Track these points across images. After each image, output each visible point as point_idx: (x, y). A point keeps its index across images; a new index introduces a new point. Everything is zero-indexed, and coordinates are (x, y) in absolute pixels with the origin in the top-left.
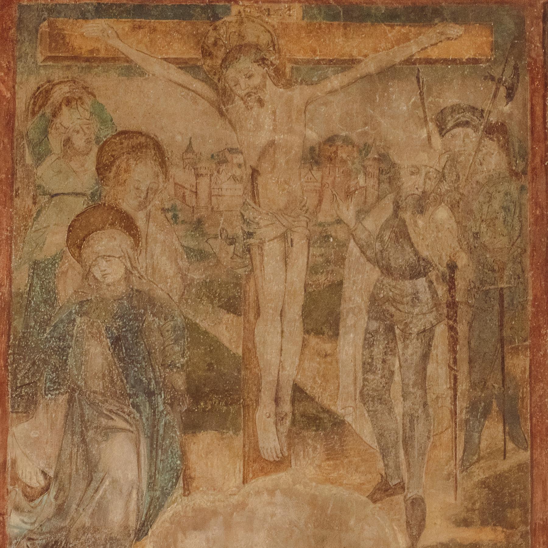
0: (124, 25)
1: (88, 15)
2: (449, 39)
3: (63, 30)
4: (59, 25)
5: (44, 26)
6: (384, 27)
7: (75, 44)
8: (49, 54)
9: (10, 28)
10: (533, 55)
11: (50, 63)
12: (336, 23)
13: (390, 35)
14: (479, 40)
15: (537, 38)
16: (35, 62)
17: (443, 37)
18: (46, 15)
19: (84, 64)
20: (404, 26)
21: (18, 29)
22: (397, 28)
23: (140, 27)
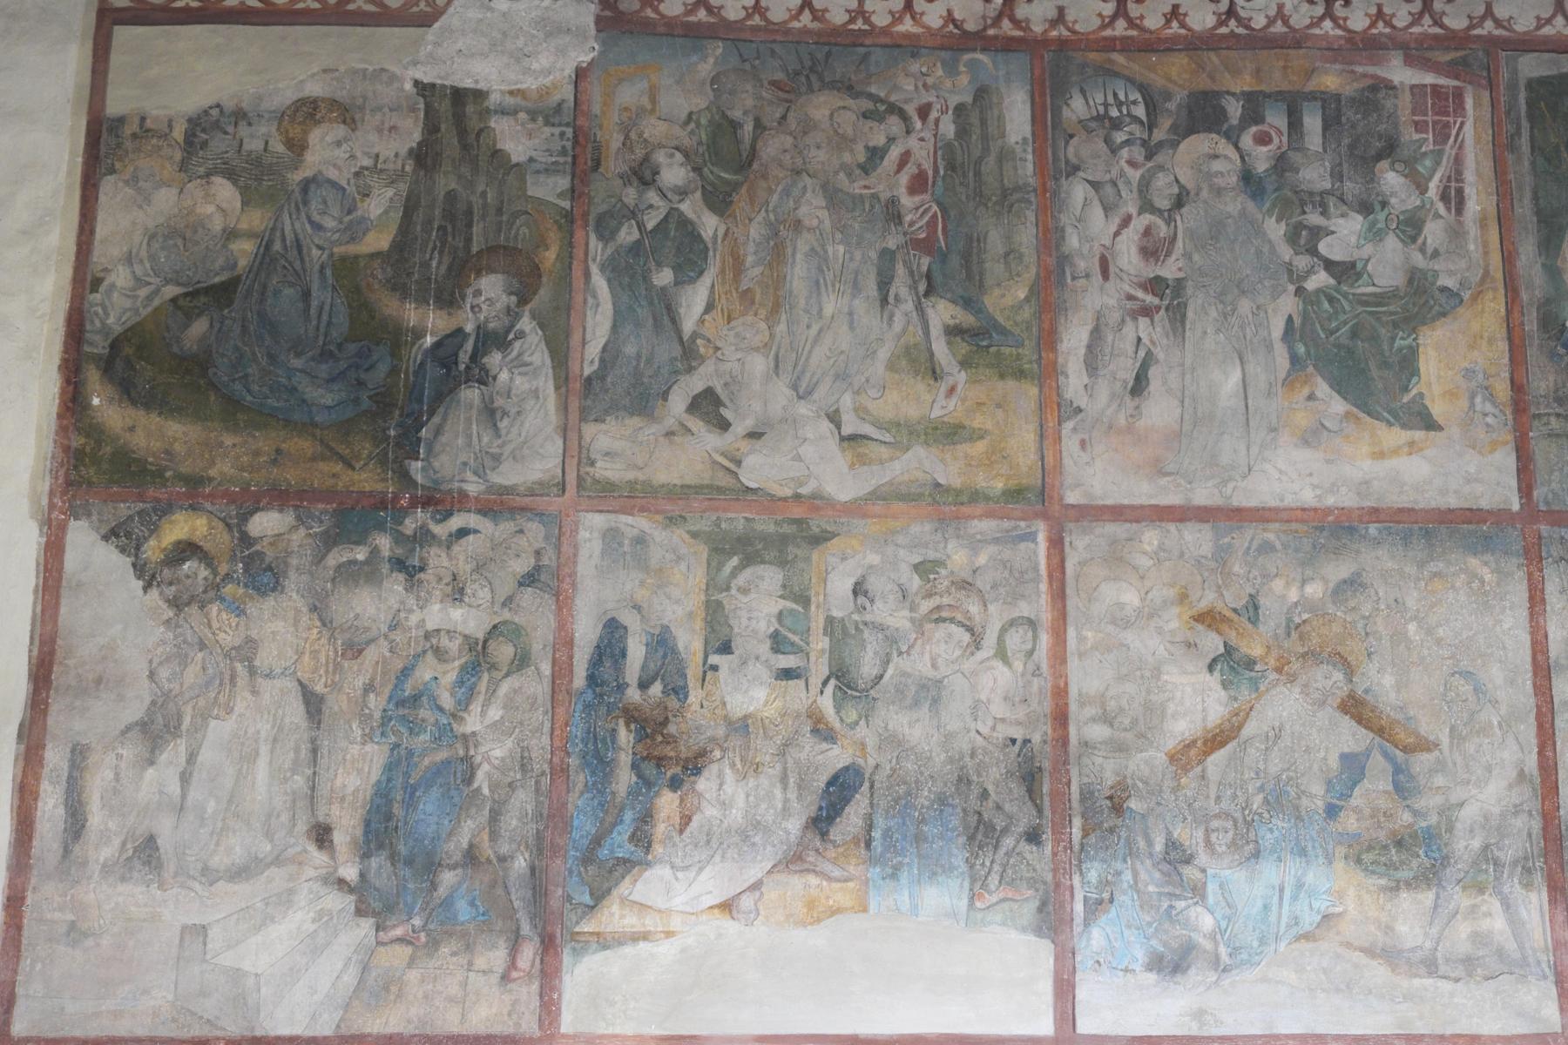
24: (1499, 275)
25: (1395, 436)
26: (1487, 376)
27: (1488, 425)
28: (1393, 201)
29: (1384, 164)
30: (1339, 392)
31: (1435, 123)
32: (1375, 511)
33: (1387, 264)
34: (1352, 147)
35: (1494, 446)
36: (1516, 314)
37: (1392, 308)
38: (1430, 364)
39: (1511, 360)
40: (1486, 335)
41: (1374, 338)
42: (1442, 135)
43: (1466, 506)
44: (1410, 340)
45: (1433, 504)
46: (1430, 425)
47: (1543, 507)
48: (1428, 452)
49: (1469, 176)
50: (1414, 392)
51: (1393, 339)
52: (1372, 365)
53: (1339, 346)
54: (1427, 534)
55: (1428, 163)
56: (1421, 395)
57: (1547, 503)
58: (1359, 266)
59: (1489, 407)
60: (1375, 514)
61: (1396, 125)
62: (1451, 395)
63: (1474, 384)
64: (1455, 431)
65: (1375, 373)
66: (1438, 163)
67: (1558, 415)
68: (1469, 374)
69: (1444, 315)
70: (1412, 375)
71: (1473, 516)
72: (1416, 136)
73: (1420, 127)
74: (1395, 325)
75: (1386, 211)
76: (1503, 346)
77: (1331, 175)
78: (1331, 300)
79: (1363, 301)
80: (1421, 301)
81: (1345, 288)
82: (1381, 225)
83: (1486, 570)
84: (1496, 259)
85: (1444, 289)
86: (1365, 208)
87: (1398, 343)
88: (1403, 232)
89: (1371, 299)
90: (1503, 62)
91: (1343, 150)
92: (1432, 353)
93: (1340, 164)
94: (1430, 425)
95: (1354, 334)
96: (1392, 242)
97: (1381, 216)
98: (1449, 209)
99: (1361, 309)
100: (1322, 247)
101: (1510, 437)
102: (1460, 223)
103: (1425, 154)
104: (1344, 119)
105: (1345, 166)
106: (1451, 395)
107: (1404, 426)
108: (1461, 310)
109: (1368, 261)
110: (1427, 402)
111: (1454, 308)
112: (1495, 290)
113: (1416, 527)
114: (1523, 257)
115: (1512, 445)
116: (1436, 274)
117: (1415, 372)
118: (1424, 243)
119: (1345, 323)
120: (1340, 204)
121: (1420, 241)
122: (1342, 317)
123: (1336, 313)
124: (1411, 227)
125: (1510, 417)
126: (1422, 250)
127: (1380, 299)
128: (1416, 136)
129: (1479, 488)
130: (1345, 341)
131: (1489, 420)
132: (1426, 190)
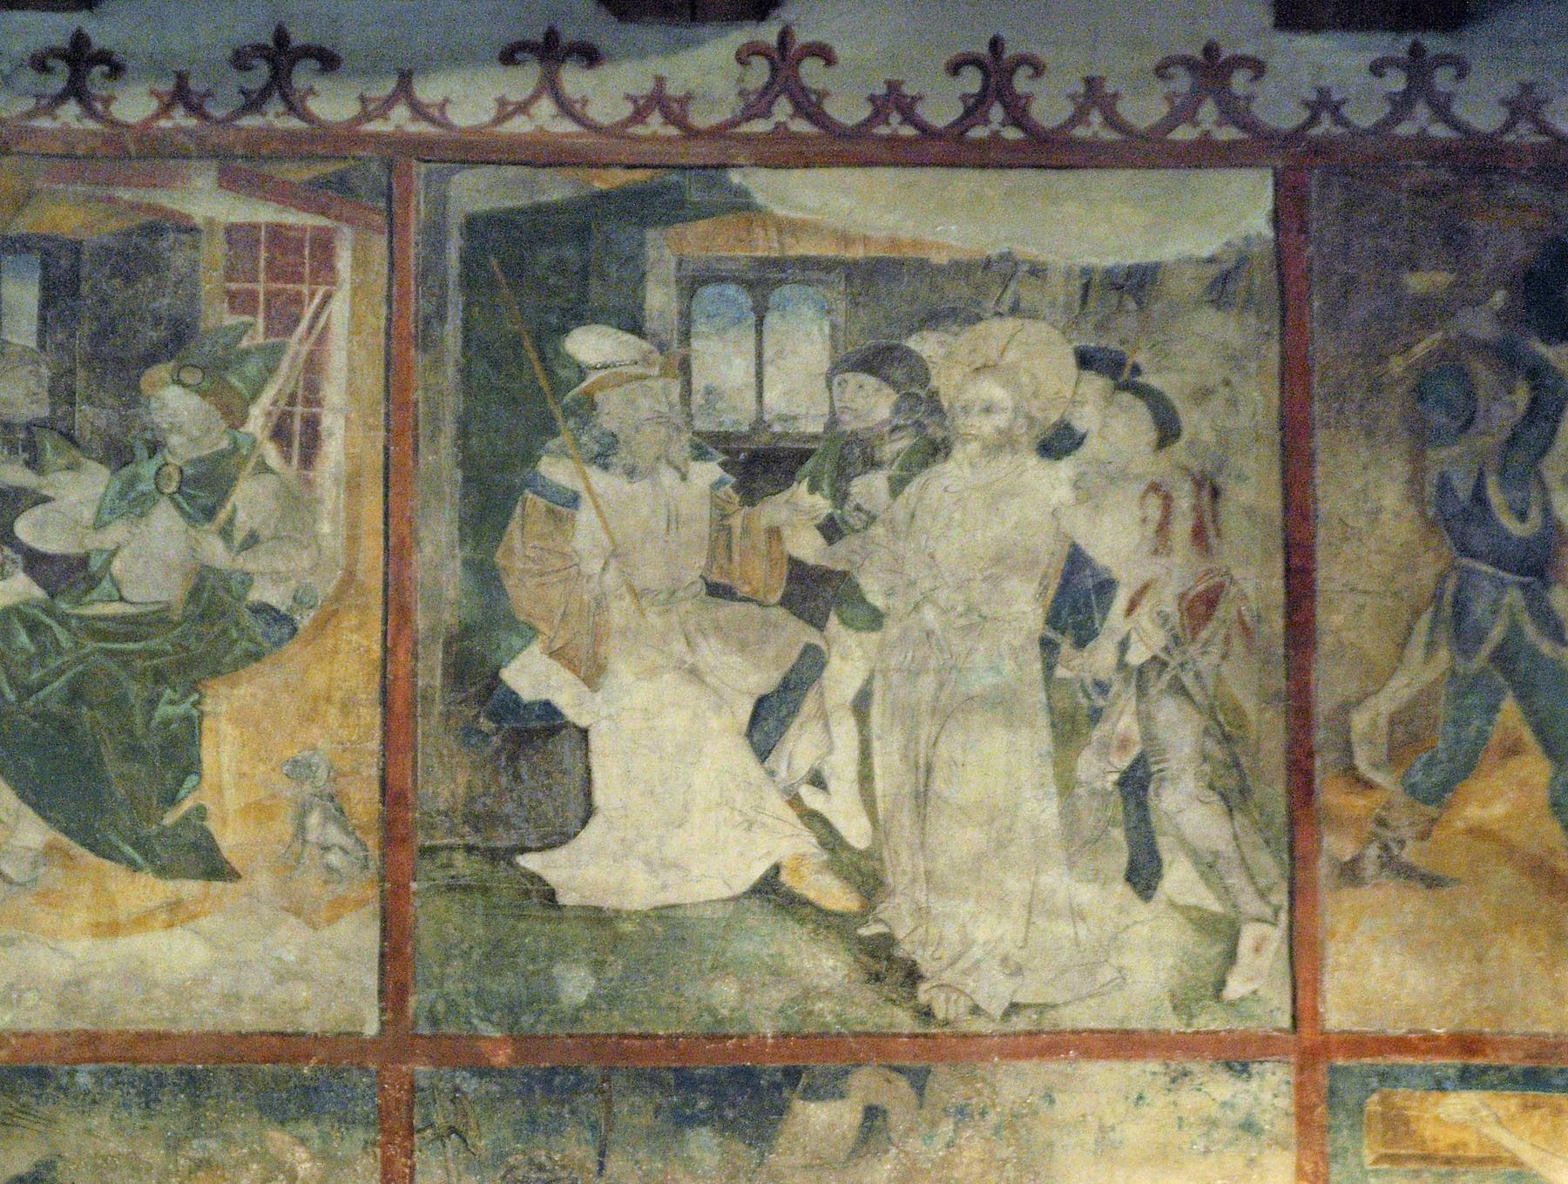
0: (1509, 1102)
1: (1448, 1084)
3: (1405, 1108)
4: (1398, 1100)
5: (1373, 1103)
7: (1427, 1133)
8: (1383, 1151)
9: (1316, 1106)
11: (1386, 1166)
16: (1361, 1165)
18: (1374, 1082)
19: (1444, 1169)
21: (1331, 1107)
23: (1535, 1107)
24: (376, 583)
25: (142, 890)
26: (335, 775)
27: (329, 868)
28: (174, 440)
29: (162, 371)
30: (36, 807)
31: (271, 296)
32: (91, 1039)
33: (151, 560)
34: (98, 337)
35: (338, 908)
36: (402, 655)
37: (154, 644)
38: (224, 753)
39: (386, 743)
40: (337, 696)
41: (119, 704)
42: (283, 317)
43: (273, 1026)
44: (187, 705)
45: (209, 1025)
46: (215, 867)
47: (424, 1029)
48: (204, 923)
49: (334, 393)
50: (187, 805)
51: (153, 703)
52: (108, 753)
53: (44, 716)
54: (192, 1082)
55: (252, 368)
56: (201, 812)
57: (434, 1021)
58: (95, 563)
59: (334, 834)
60: (90, 1043)
61: (193, 299)
62: (259, 811)
63: (307, 788)
64: (263, 881)
65: (113, 767)
66: (271, 370)
67: (470, 849)
68: (299, 770)
69: (256, 656)
70: (187, 772)
71: (286, 1045)
72: (230, 320)
73: (241, 302)
74: (159, 677)
75: (158, 460)
76: (371, 716)
77: (51, 392)
78: (33, 628)
79: (97, 630)
80: (216, 630)
81: (63, 606)
82: (146, 486)
83: (301, 1153)
84: (372, 549)
85: (261, 609)
86: (118, 455)
87: (164, 710)
88: (191, 499)
89: (112, 626)
90: (419, 184)
91: (81, 345)
92: (227, 728)
93: (72, 372)
94: (215, 867)
95: (75, 694)
96: (165, 520)
97: (148, 469)
98: (287, 458)
99: (90, 645)
100: (24, 529)
101: (373, 893)
102: (309, 483)
103: (247, 352)
104: (85, 288)
105: (81, 374)
106: (259, 811)
107: (163, 872)
108: (291, 648)
109: (114, 554)
110: (212, 825)
111: (278, 644)
112: (364, 609)
113: (170, 1069)
114: (428, 549)
115: (374, 907)
116: (247, 580)
117: (192, 767)
118: (231, 521)
119: (60, 672)
120: (63, 444)
121: (222, 515)
122: (53, 663)
123: (43, 653)
124: (205, 490)
125: (375, 853)
126: (226, 534)
127: (133, 627)
128: (230, 320)
129: (303, 993)
130: (54, 707)
131: (334, 858)
132: (244, 419)
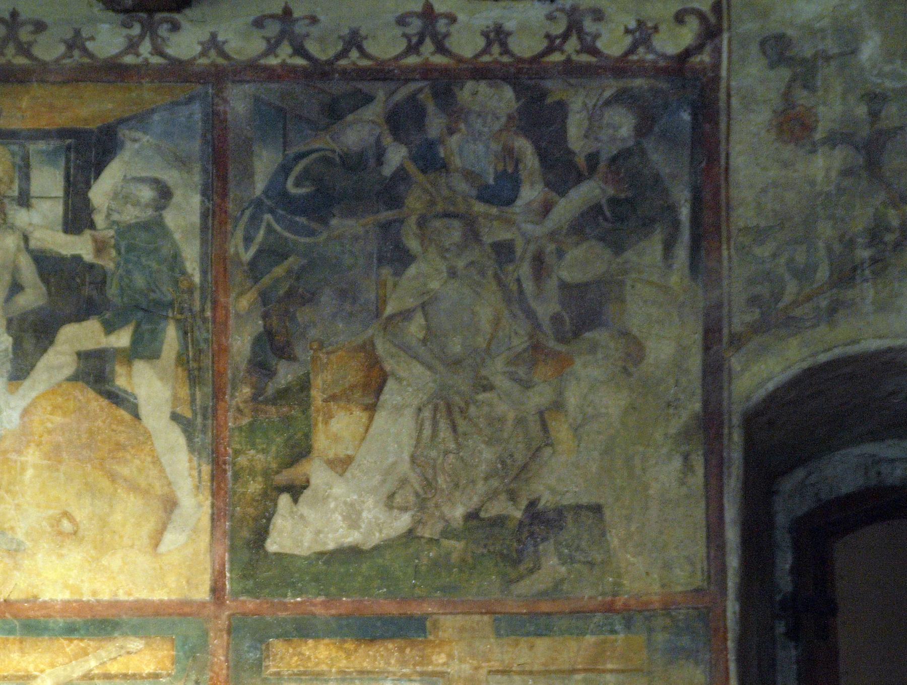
2: (129, 653)
6: (63, 642)
10: (216, 669)
12: (11, 637)
13: (68, 650)
14: (160, 654)
15: (220, 651)
17: (123, 651)
20: (82, 640)
22: (76, 642)
